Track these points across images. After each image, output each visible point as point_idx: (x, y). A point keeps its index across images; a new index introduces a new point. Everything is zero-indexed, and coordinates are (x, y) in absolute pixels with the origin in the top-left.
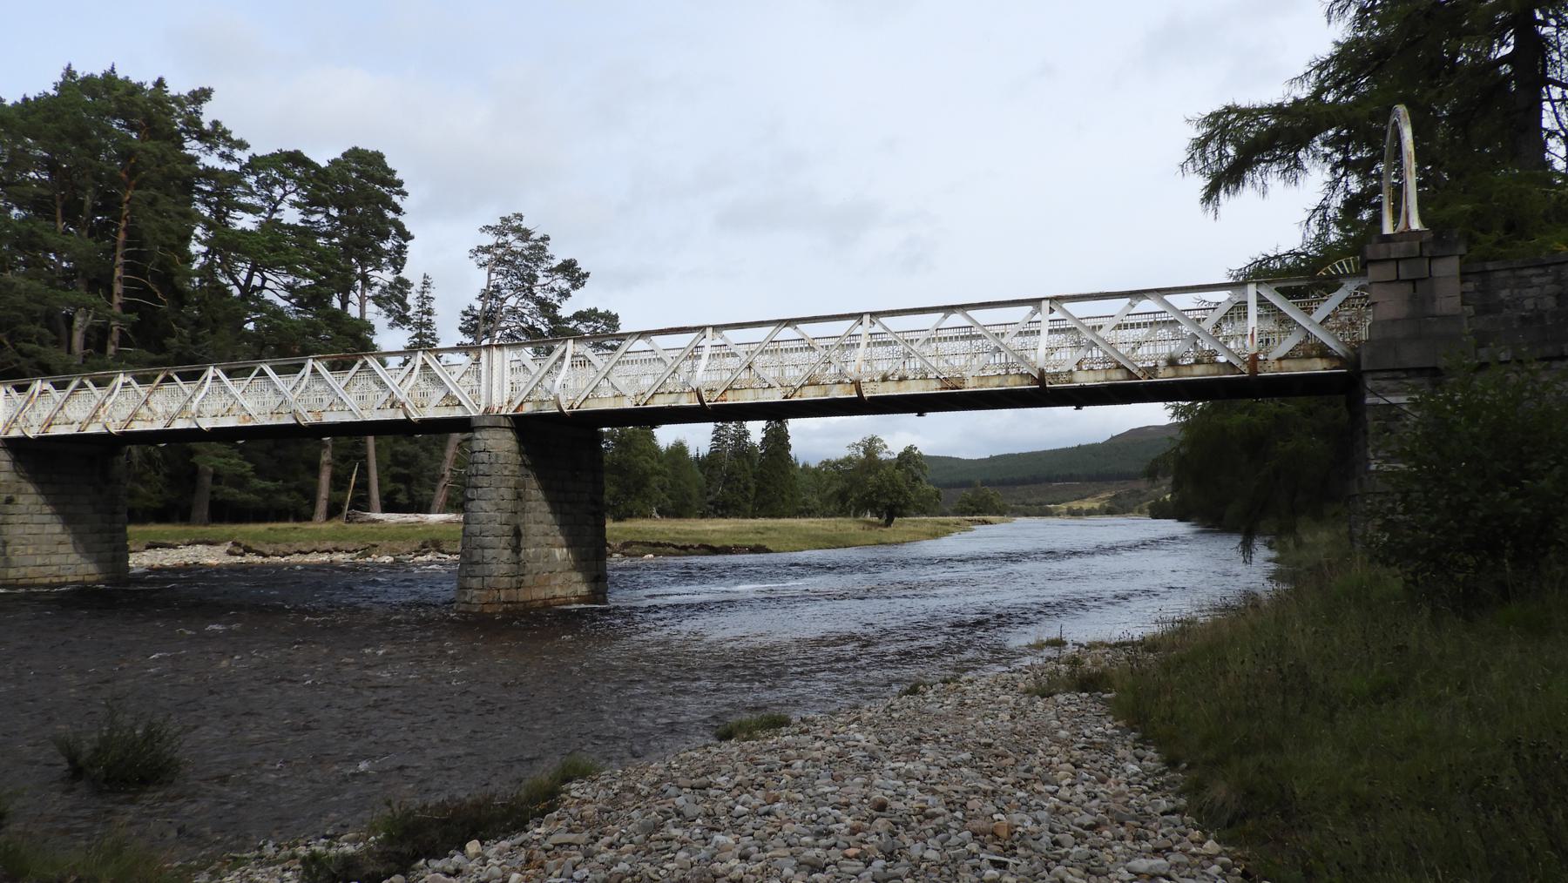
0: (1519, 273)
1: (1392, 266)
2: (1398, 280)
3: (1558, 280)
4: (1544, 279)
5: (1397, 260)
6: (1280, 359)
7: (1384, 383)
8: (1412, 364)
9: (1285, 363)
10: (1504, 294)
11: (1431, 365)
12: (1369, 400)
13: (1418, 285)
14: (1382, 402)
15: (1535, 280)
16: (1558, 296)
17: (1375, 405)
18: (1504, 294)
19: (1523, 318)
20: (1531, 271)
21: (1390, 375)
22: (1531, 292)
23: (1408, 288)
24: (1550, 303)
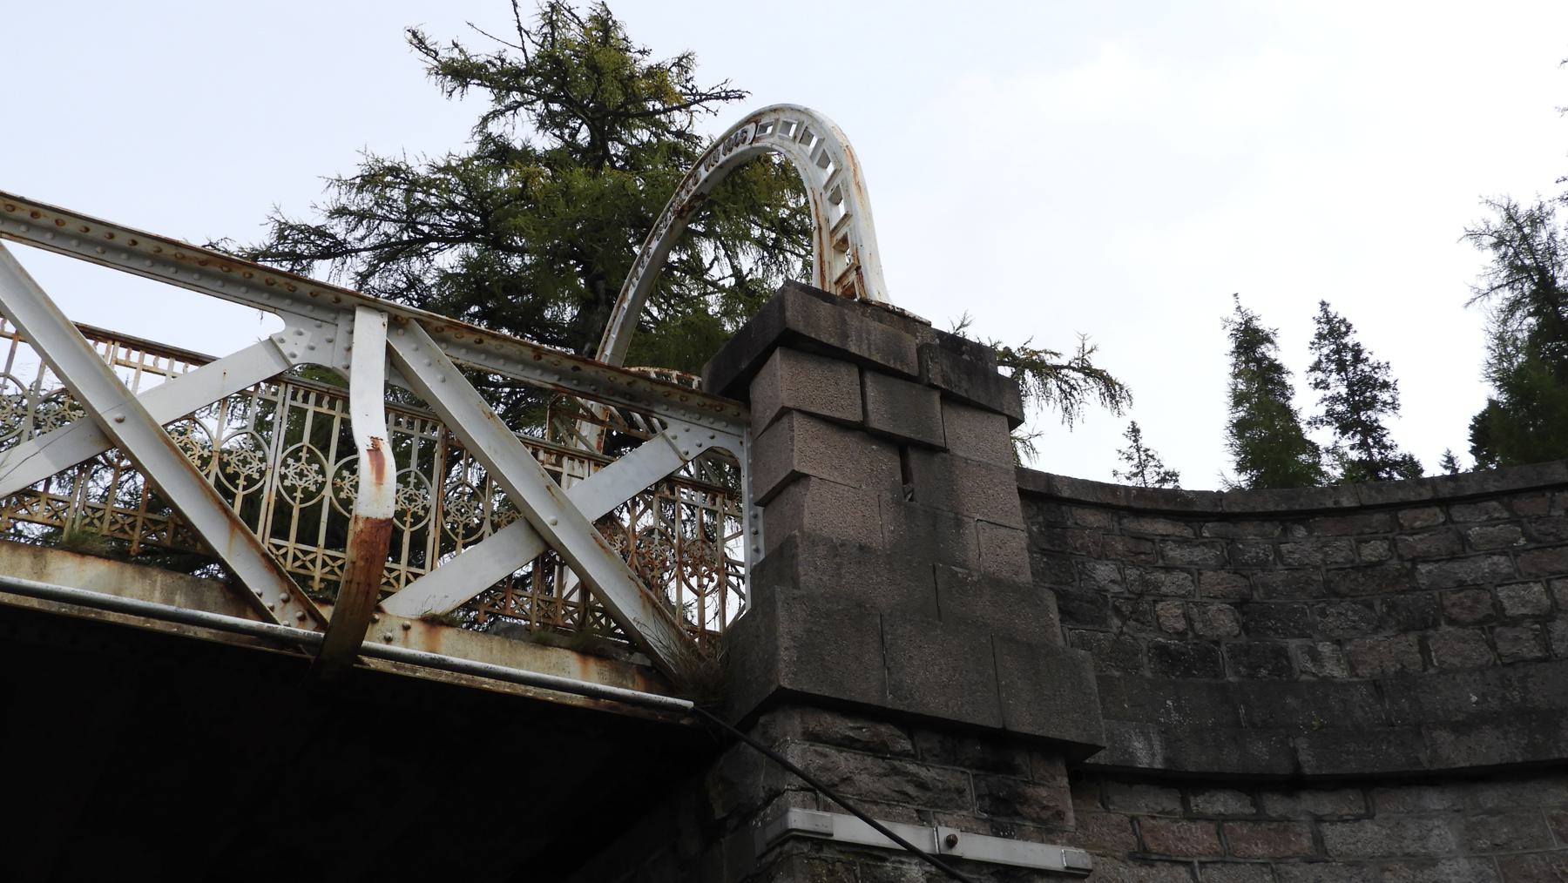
0: (1131, 524)
1: (847, 377)
2: (860, 429)
3: (1231, 562)
4: (1197, 554)
5: (864, 366)
6: (433, 622)
7: (844, 762)
8: (937, 705)
9: (447, 635)
10: (1104, 572)
11: (986, 718)
12: (800, 818)
13: (915, 459)
14: (850, 829)
15: (1175, 553)
16: (1241, 604)
17: (822, 841)
18: (1104, 572)
19: (1162, 651)
20: (1161, 527)
21: (865, 732)
22: (1169, 582)
23: (888, 462)
24: (1225, 622)
